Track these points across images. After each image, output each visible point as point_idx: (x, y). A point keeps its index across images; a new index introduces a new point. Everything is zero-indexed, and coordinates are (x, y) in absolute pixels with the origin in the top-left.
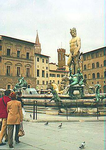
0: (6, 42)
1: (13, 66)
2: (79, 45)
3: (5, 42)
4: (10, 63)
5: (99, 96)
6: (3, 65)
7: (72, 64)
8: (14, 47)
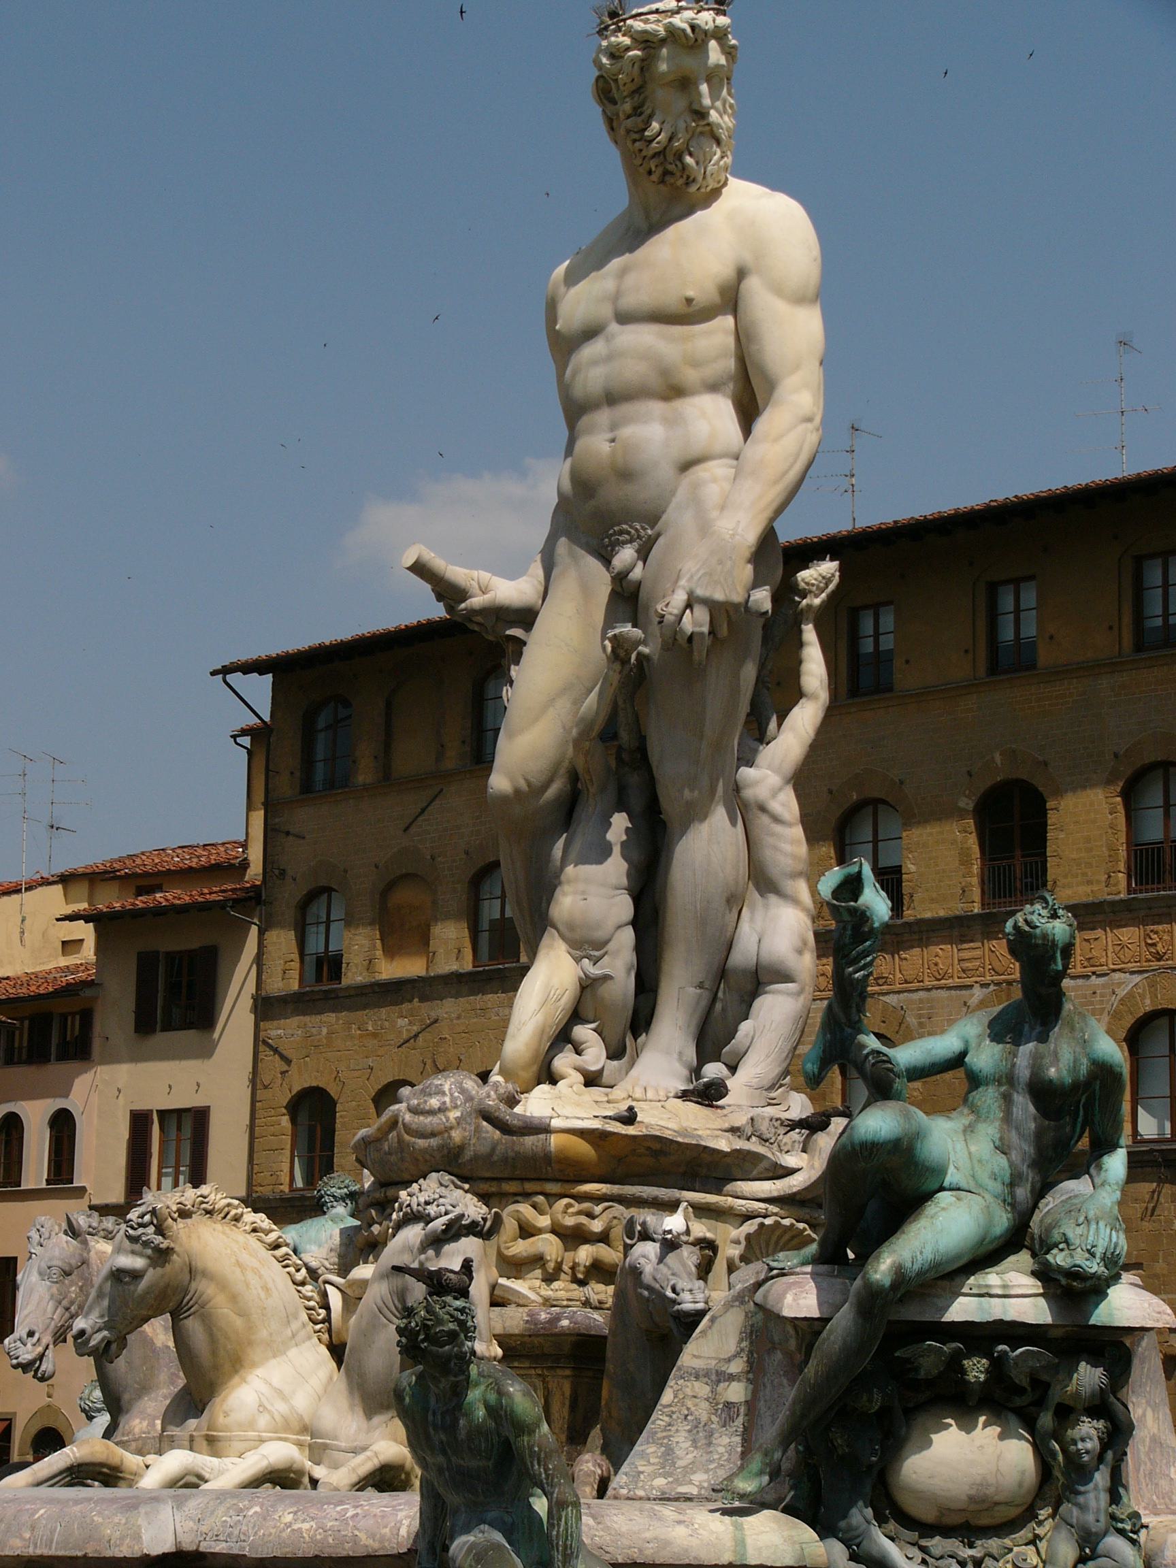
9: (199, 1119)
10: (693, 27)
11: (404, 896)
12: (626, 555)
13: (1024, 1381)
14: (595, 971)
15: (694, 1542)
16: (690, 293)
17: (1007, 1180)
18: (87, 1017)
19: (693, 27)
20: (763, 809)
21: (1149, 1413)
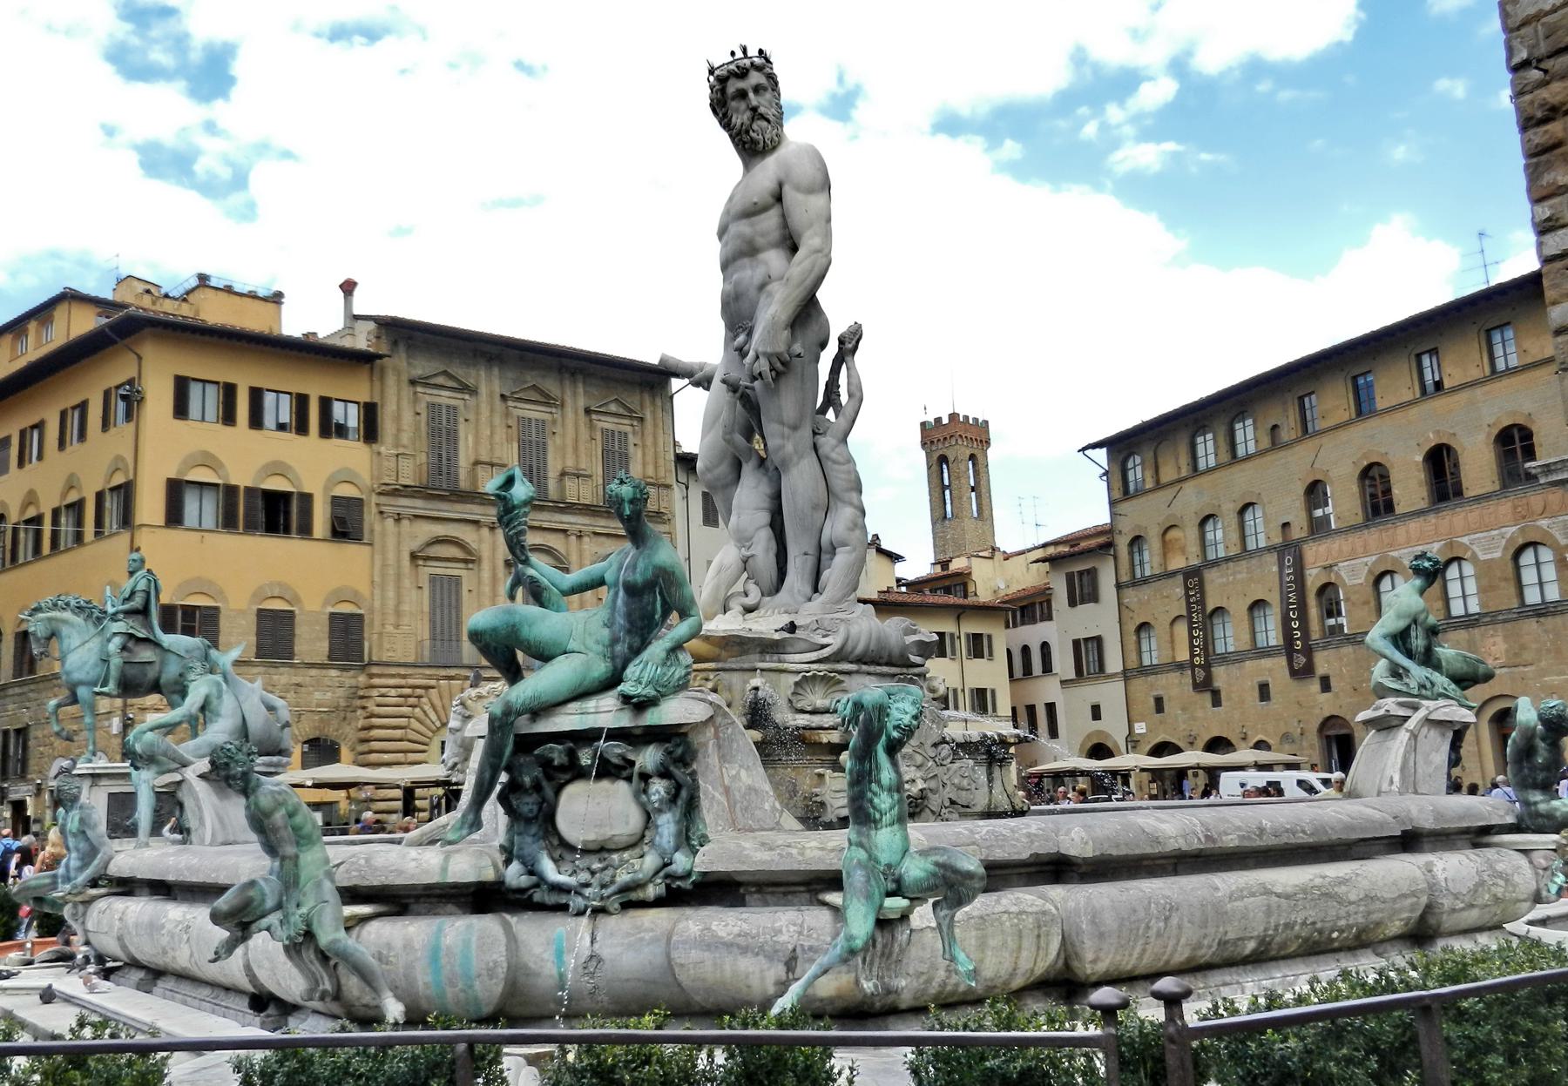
0: (418, 371)
1: (486, 575)
2: (808, 243)
3: (402, 365)
4: (453, 552)
5: (884, 858)
6: (399, 561)
7: (748, 469)
8: (492, 411)
9: (1098, 640)
10: (738, 67)
11: (1172, 534)
12: (741, 338)
13: (615, 760)
14: (749, 553)
15: (418, 871)
16: (755, 200)
17: (607, 642)
18: (1049, 602)
19: (738, 67)
20: (828, 458)
21: (743, 773)
